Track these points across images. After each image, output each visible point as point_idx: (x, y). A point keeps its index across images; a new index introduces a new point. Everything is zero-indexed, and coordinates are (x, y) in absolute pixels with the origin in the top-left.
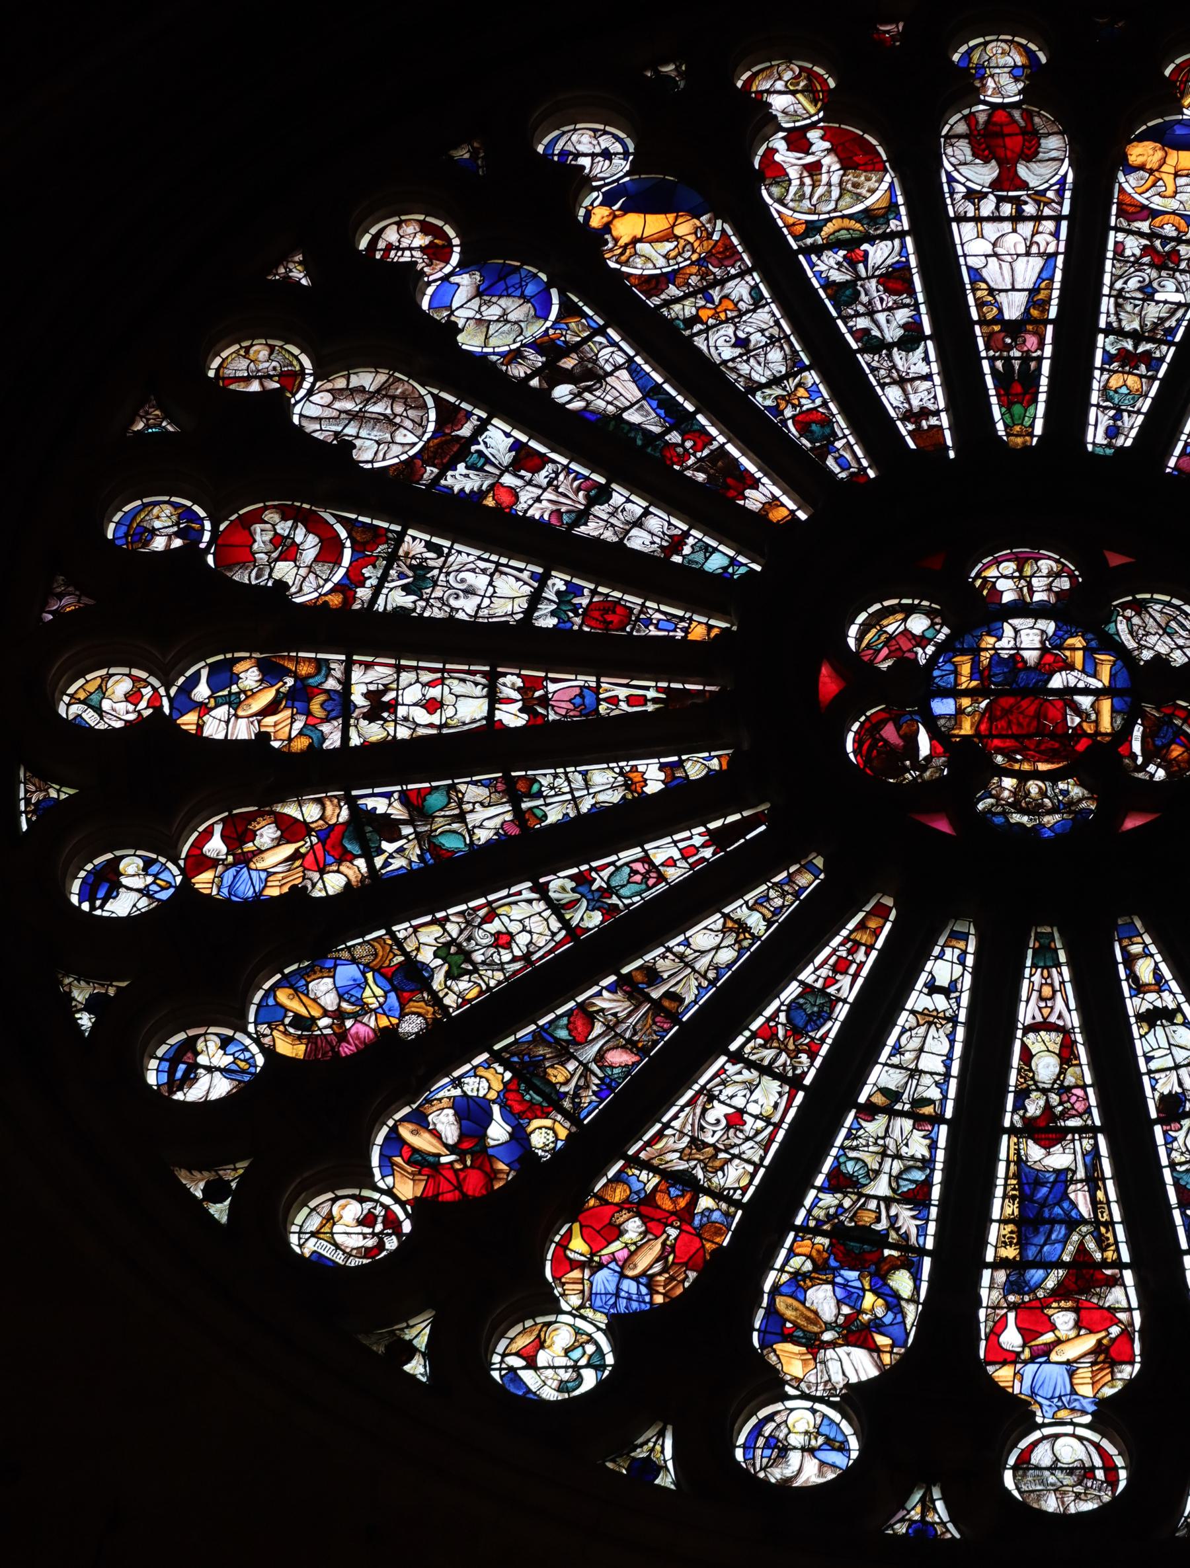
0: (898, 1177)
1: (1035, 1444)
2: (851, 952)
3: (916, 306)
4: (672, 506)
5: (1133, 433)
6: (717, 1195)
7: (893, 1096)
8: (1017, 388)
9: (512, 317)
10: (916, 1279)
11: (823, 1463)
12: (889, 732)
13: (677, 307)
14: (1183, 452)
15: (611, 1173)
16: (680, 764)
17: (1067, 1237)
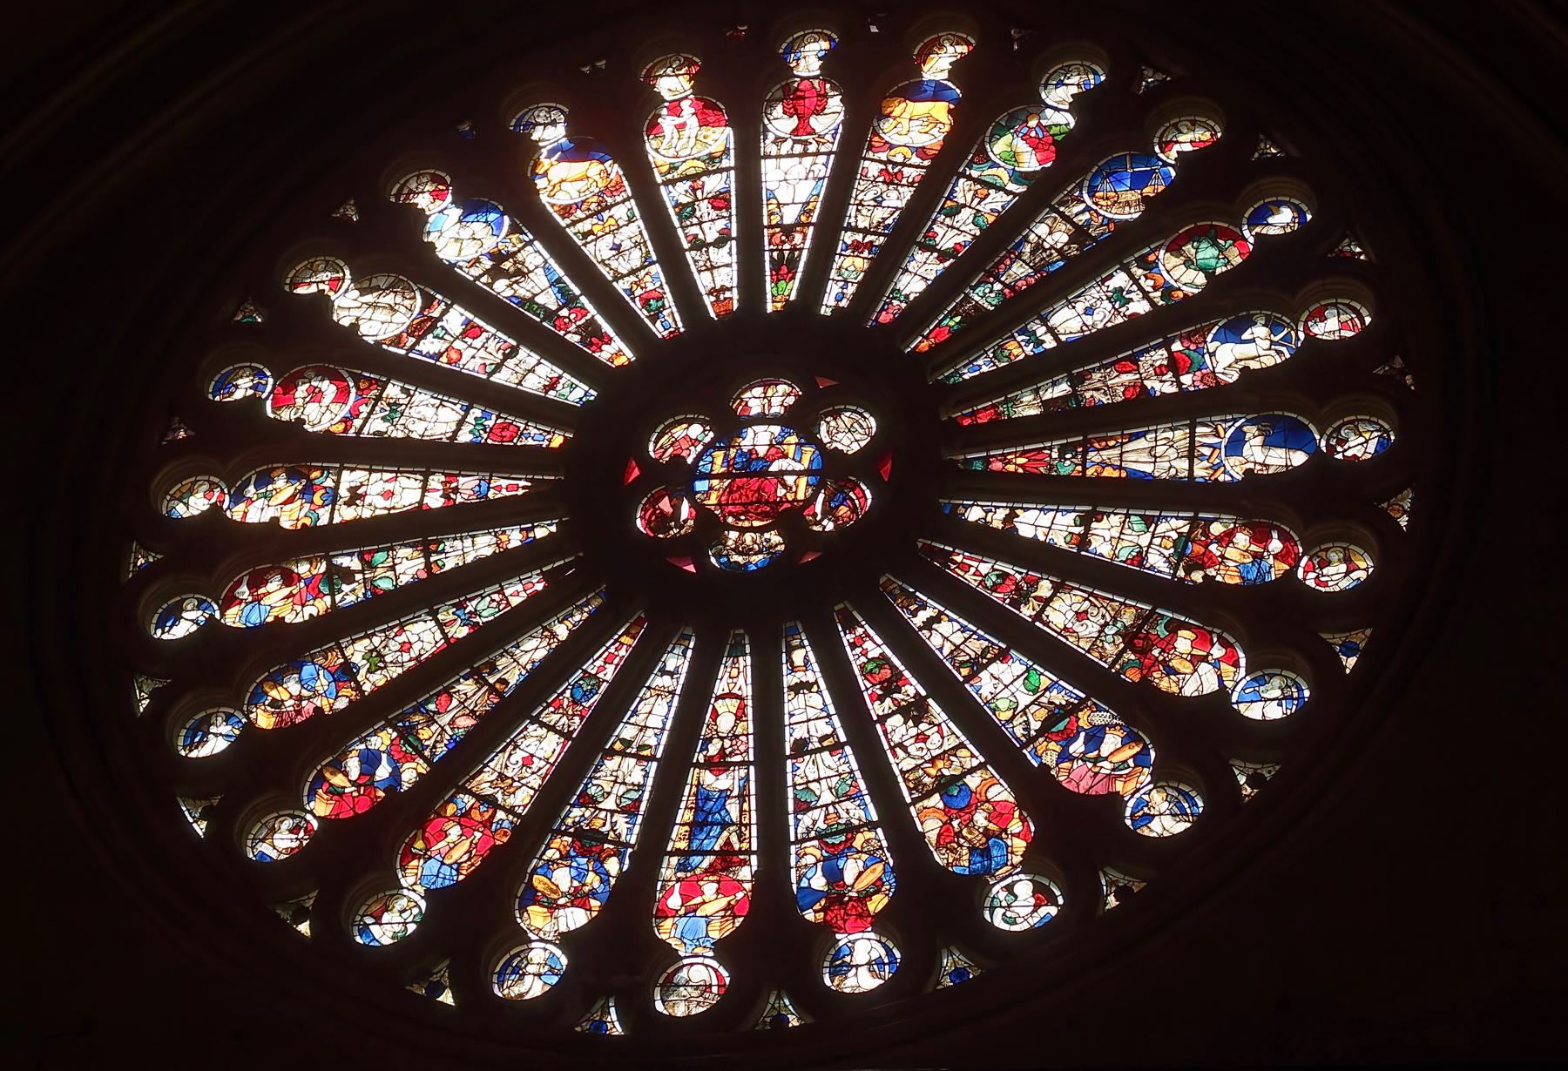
4: (555, 360)
8: (784, 269)
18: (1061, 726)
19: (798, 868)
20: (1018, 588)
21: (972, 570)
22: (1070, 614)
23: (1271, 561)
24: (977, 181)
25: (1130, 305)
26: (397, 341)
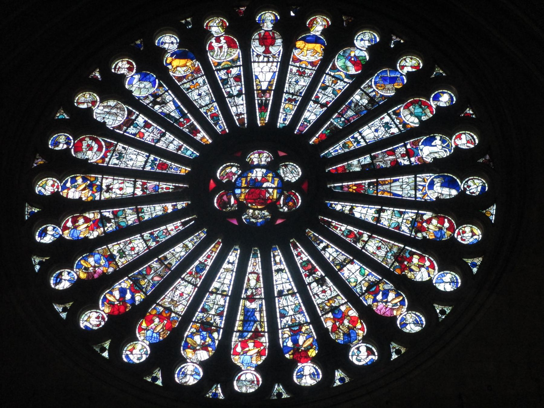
0: (217, 310)
1: (242, 375)
2: (211, 253)
3: (242, 85)
4: (180, 138)
5: (289, 120)
6: (176, 313)
7: (217, 289)
8: (263, 108)
9: (147, 87)
10: (219, 334)
11: (194, 378)
12: (225, 198)
13: (185, 85)
14: (301, 126)
15: (153, 307)
16: (176, 205)
17: (254, 325)
18: (373, 289)
19: (282, 338)
20: (356, 236)
21: (339, 229)
22: (375, 247)
23: (445, 230)
24: (333, 77)
25: (391, 129)
26: (119, 127)
